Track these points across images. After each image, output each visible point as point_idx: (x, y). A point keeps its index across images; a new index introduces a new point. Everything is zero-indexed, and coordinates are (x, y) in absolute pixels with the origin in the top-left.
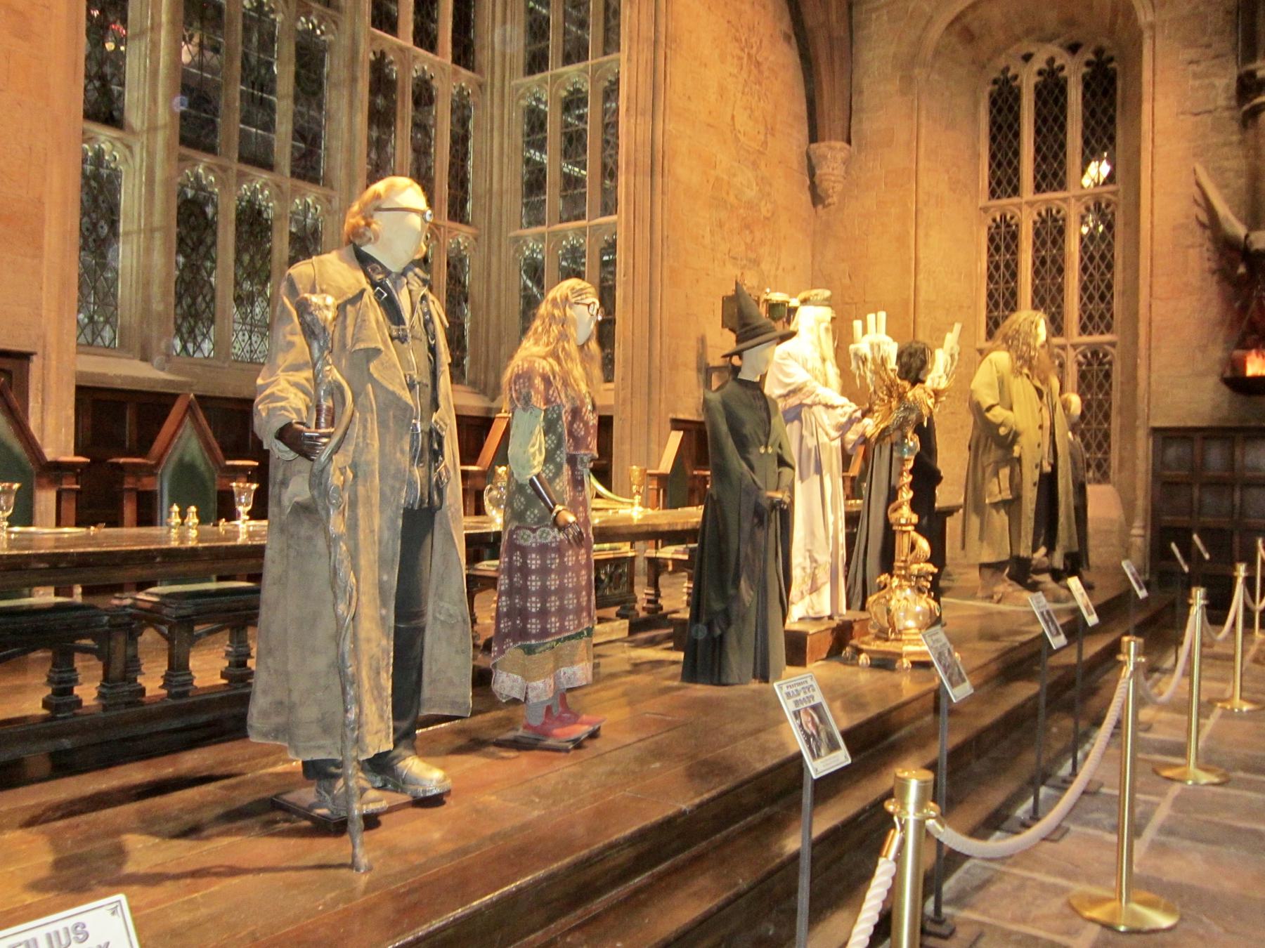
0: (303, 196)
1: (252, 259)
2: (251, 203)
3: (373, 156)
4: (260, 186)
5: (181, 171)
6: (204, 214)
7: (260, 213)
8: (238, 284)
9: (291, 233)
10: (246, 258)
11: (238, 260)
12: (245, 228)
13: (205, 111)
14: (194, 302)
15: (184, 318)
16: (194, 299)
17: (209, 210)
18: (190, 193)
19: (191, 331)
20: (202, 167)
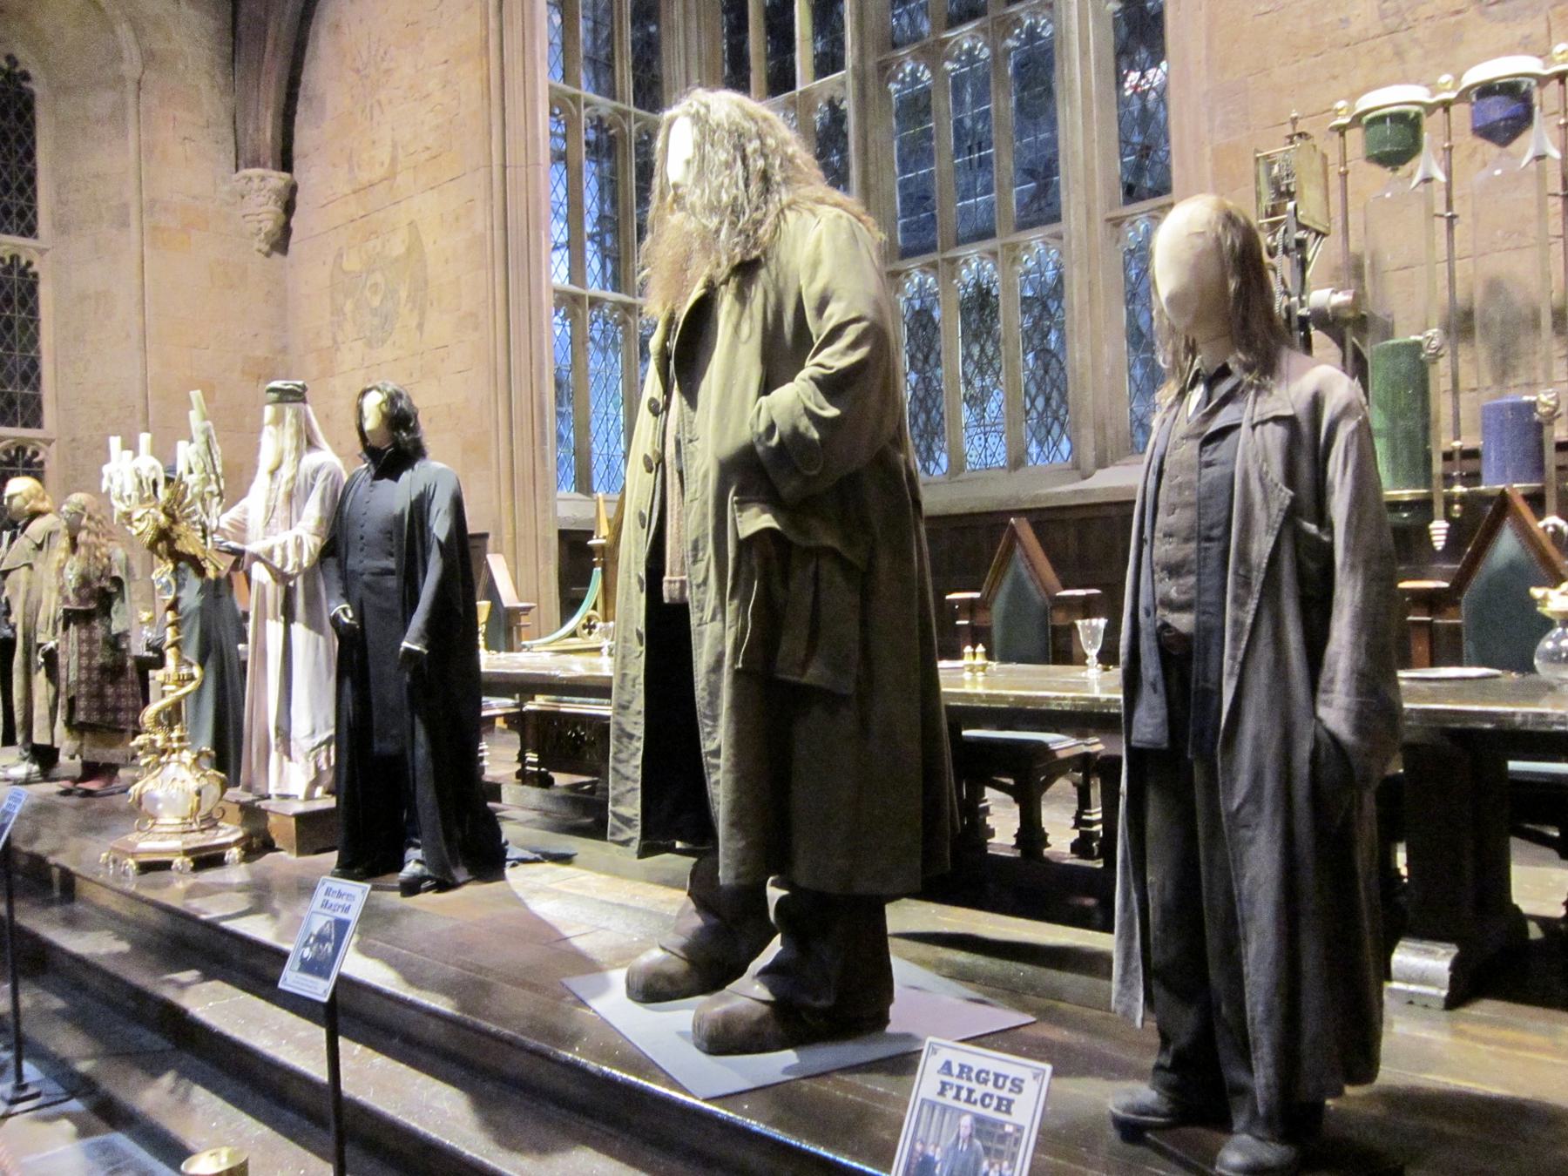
0: (1027, 248)
1: (982, 350)
2: (978, 285)
3: (1136, 138)
4: (975, 263)
5: (898, 289)
6: (931, 318)
7: (988, 292)
8: (968, 383)
9: (1024, 299)
10: (976, 351)
11: (968, 356)
12: (974, 316)
13: (926, 210)
14: (928, 418)
15: (921, 437)
16: (928, 413)
17: (937, 314)
18: (917, 304)
19: (929, 449)
20: (917, 277)
